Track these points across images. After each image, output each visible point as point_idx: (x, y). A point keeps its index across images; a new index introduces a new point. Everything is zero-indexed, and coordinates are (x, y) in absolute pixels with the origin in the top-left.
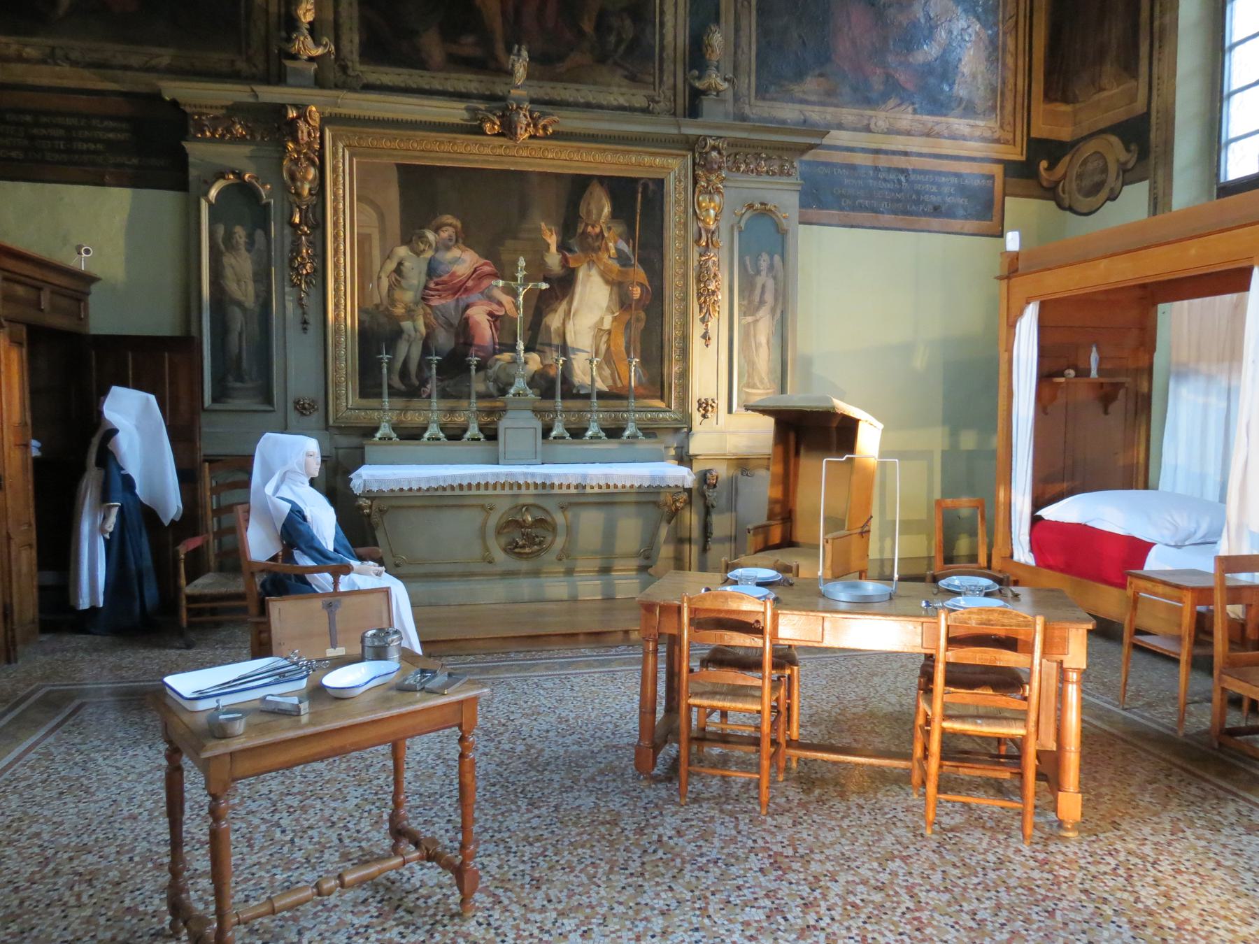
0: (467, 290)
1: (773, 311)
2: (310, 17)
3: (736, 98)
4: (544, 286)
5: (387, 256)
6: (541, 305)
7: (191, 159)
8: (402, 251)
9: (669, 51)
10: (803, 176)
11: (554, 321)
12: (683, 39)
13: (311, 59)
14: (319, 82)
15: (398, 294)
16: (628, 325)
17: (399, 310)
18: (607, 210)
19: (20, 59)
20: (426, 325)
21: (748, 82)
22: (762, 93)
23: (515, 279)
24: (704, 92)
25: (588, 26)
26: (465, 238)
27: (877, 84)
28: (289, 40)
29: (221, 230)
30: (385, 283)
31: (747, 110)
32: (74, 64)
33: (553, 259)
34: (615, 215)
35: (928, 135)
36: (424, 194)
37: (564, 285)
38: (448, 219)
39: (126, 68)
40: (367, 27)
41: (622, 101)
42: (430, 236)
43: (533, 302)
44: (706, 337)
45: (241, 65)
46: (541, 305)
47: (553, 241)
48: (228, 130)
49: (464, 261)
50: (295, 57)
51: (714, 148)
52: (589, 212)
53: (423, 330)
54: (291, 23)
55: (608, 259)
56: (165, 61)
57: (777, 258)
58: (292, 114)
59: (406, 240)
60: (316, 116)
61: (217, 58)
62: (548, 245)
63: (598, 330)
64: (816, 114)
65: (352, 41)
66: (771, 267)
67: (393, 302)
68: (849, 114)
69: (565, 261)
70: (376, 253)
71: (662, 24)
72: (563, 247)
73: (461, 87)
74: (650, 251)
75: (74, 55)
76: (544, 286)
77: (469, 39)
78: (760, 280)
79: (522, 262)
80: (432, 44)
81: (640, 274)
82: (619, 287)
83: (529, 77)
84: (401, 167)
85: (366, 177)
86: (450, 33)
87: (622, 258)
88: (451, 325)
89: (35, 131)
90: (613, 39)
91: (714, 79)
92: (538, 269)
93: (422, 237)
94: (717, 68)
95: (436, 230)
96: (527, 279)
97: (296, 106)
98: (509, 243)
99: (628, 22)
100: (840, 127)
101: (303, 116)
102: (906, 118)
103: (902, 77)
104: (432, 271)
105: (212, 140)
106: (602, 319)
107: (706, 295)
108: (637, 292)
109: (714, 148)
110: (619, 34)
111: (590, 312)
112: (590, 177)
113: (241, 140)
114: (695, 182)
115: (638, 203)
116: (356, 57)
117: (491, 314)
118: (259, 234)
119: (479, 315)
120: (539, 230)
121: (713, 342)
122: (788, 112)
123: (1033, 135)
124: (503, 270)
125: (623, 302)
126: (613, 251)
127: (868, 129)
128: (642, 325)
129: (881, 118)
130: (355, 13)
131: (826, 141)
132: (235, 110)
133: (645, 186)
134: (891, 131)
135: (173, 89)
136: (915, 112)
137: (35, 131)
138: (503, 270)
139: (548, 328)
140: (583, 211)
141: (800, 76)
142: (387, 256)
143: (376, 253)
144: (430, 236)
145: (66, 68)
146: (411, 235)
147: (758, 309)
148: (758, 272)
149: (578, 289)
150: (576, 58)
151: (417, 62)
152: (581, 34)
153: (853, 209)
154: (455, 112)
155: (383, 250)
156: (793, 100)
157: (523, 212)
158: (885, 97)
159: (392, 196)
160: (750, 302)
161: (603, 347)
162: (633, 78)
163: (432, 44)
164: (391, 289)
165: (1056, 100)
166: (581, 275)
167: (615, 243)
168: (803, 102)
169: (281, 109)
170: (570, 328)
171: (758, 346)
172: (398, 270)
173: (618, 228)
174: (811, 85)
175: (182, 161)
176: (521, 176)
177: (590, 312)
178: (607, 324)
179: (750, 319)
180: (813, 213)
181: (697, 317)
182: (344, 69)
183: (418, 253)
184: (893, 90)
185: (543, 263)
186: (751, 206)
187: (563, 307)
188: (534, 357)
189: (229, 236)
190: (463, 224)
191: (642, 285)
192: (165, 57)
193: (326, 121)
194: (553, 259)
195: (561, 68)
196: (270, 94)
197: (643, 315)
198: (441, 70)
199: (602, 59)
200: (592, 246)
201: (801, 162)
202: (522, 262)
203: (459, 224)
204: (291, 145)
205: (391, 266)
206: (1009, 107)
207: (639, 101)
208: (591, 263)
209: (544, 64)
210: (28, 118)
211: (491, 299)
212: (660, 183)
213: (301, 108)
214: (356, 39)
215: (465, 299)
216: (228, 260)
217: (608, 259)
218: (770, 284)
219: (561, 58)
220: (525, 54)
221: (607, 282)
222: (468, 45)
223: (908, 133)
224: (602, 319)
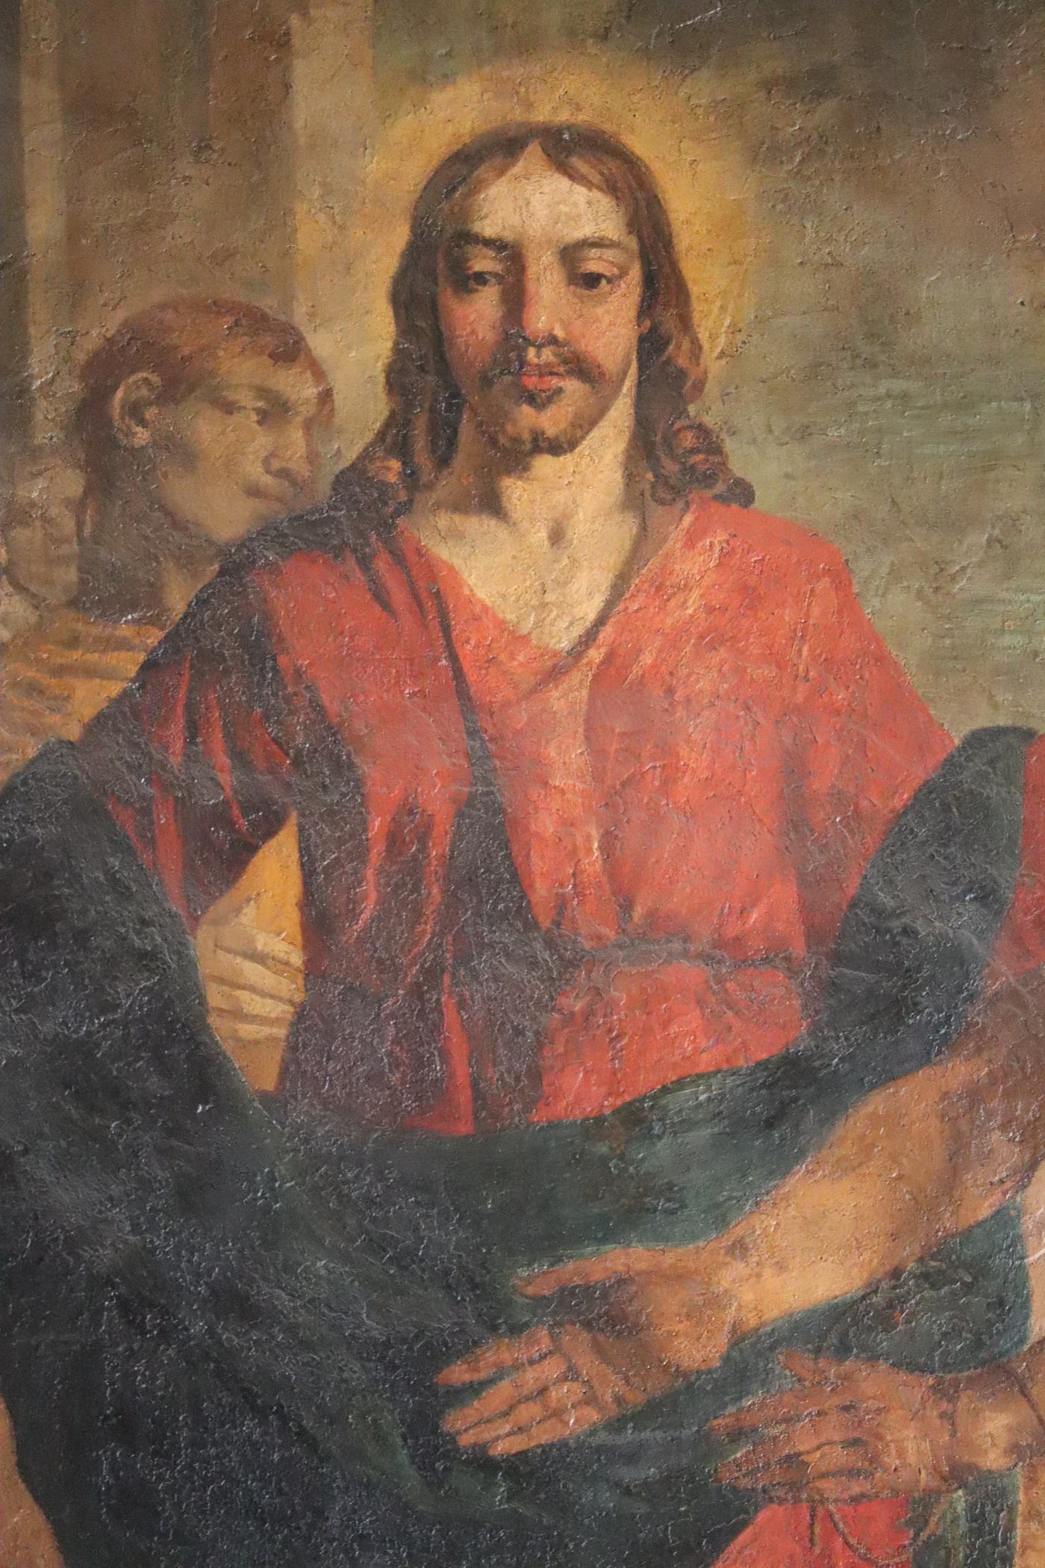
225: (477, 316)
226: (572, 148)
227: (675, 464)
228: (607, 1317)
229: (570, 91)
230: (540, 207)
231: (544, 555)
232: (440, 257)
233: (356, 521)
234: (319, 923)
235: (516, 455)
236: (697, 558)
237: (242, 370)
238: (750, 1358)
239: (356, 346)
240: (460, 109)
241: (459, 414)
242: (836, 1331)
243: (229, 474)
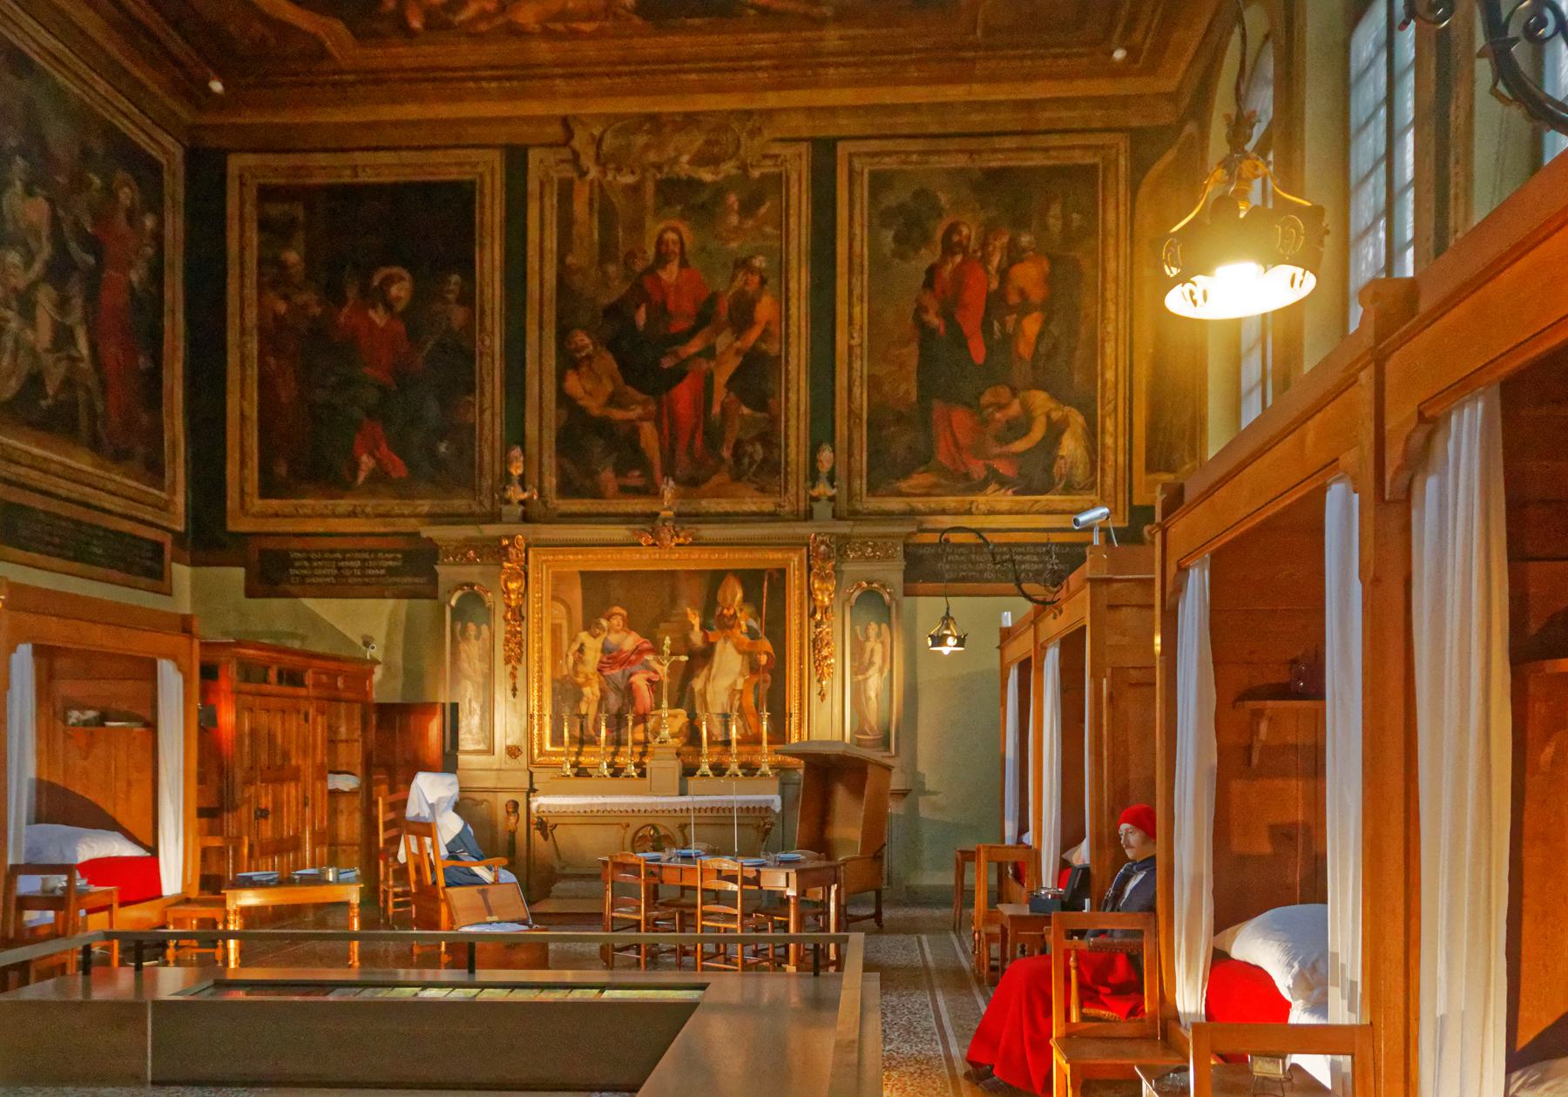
0: (631, 663)
1: (881, 671)
2: (520, 471)
3: (850, 497)
4: (684, 658)
5: (573, 640)
6: (686, 674)
7: (441, 579)
8: (584, 636)
9: (792, 467)
10: (906, 555)
11: (698, 684)
12: (804, 457)
13: (522, 502)
14: (526, 518)
15: (580, 668)
16: (757, 686)
17: (581, 680)
18: (739, 595)
19: (334, 515)
20: (601, 690)
21: (860, 484)
22: (873, 490)
23: (662, 653)
24: (815, 499)
25: (726, 453)
26: (631, 625)
27: (978, 470)
28: (505, 489)
29: (459, 626)
30: (571, 659)
31: (859, 507)
32: (367, 516)
33: (697, 637)
34: (746, 599)
35: (1028, 513)
36: (599, 592)
37: (702, 657)
38: (617, 609)
39: (402, 516)
40: (562, 473)
41: (754, 508)
42: (604, 623)
43: (681, 671)
44: (822, 695)
45: (476, 508)
46: (686, 674)
47: (696, 621)
48: (465, 555)
49: (630, 641)
50: (508, 502)
51: (822, 542)
52: (725, 599)
53: (598, 693)
54: (507, 476)
55: (740, 633)
56: (426, 509)
57: (884, 626)
58: (506, 542)
59: (587, 627)
60: (522, 542)
61: (460, 504)
62: (692, 626)
63: (733, 691)
64: (919, 504)
65: (551, 481)
66: (879, 635)
67: (576, 673)
68: (950, 502)
69: (706, 637)
70: (565, 636)
71: (787, 445)
72: (704, 627)
73: (629, 509)
74: (775, 629)
75: (369, 510)
76: (684, 658)
77: (637, 473)
78: (869, 645)
79: (668, 641)
80: (607, 476)
81: (766, 645)
82: (750, 657)
83: (677, 496)
84: (582, 573)
85: (559, 579)
86: (620, 472)
87: (752, 633)
88: (617, 689)
89: (342, 564)
90: (746, 461)
91: (823, 489)
92: (683, 644)
93: (598, 625)
94: (831, 479)
95: (608, 619)
96: (672, 654)
97: (508, 537)
98: (662, 625)
99: (759, 447)
100: (943, 512)
101: (512, 545)
102: (1005, 499)
103: (1003, 468)
104: (605, 650)
105: (455, 564)
106: (735, 683)
107: (819, 662)
108: (764, 659)
109: (822, 542)
110: (751, 456)
111: (727, 674)
112: (727, 571)
113: (470, 562)
114: (810, 569)
115: (764, 589)
116: (553, 495)
117: (649, 680)
118: (484, 628)
119: (640, 681)
120: (686, 615)
121: (828, 698)
122: (895, 504)
123: (1135, 503)
124: (656, 650)
125: (754, 668)
126: (744, 628)
127: (969, 512)
128: (768, 685)
129: (981, 501)
130: (553, 462)
131: (926, 526)
132: (469, 543)
133: (771, 575)
134: (991, 512)
135: (427, 532)
136: (1015, 493)
137: (342, 564)
138: (656, 650)
139: (692, 690)
140: (720, 598)
141: (906, 474)
142: (573, 640)
143: (565, 636)
144: (604, 623)
145: (362, 520)
146: (590, 625)
147: (867, 669)
148: (867, 639)
149: (717, 658)
150: (715, 479)
151: (598, 495)
152: (723, 460)
153: (956, 580)
154: (619, 532)
155: (570, 633)
156: (900, 494)
157: (674, 600)
158: (981, 487)
159: (576, 596)
160: (861, 663)
161: (737, 703)
162: (762, 490)
163: (607, 476)
164: (575, 664)
165: (1159, 471)
166: (719, 647)
167: (745, 621)
168: (908, 495)
169: (499, 539)
170: (710, 688)
171: (868, 699)
172: (581, 650)
173: (748, 609)
174: (919, 480)
175: (434, 577)
176: (672, 573)
177: (727, 674)
178: (740, 686)
179: (860, 677)
180: (921, 586)
181: (814, 679)
182: (545, 503)
183: (595, 637)
184: (995, 478)
185: (687, 639)
186: (859, 586)
187: (705, 671)
188: (682, 714)
189: (464, 630)
190: (629, 615)
191: (768, 654)
192: (425, 506)
193: (528, 546)
194: (697, 637)
195: (705, 487)
196: (491, 530)
197: (769, 677)
198: (614, 497)
199: (737, 478)
200: (727, 624)
201: (906, 545)
202: (668, 641)
203: (624, 612)
204: (506, 564)
205: (576, 647)
206: (1109, 480)
207: (768, 505)
208: (726, 639)
209: (691, 484)
210: (339, 556)
211: (648, 668)
212: (782, 572)
213: (512, 538)
214: (554, 481)
215: (630, 669)
216: (463, 647)
217: (740, 633)
218: (878, 648)
219: (705, 481)
220: (671, 483)
221: (739, 652)
222: (635, 478)
223: (1010, 513)
224: (735, 683)
225: (664, 248)
226: (675, 230)
227: (684, 264)
228: (676, 354)
229: (674, 223)
230: (671, 236)
231: (670, 274)
232: (660, 242)
233: (651, 271)
234: (648, 313)
235: (667, 262)
236: (684, 272)
237: (640, 255)
238: (689, 358)
239: (651, 252)
240: (662, 226)
241: (662, 258)
242: (699, 354)
243: (639, 266)
